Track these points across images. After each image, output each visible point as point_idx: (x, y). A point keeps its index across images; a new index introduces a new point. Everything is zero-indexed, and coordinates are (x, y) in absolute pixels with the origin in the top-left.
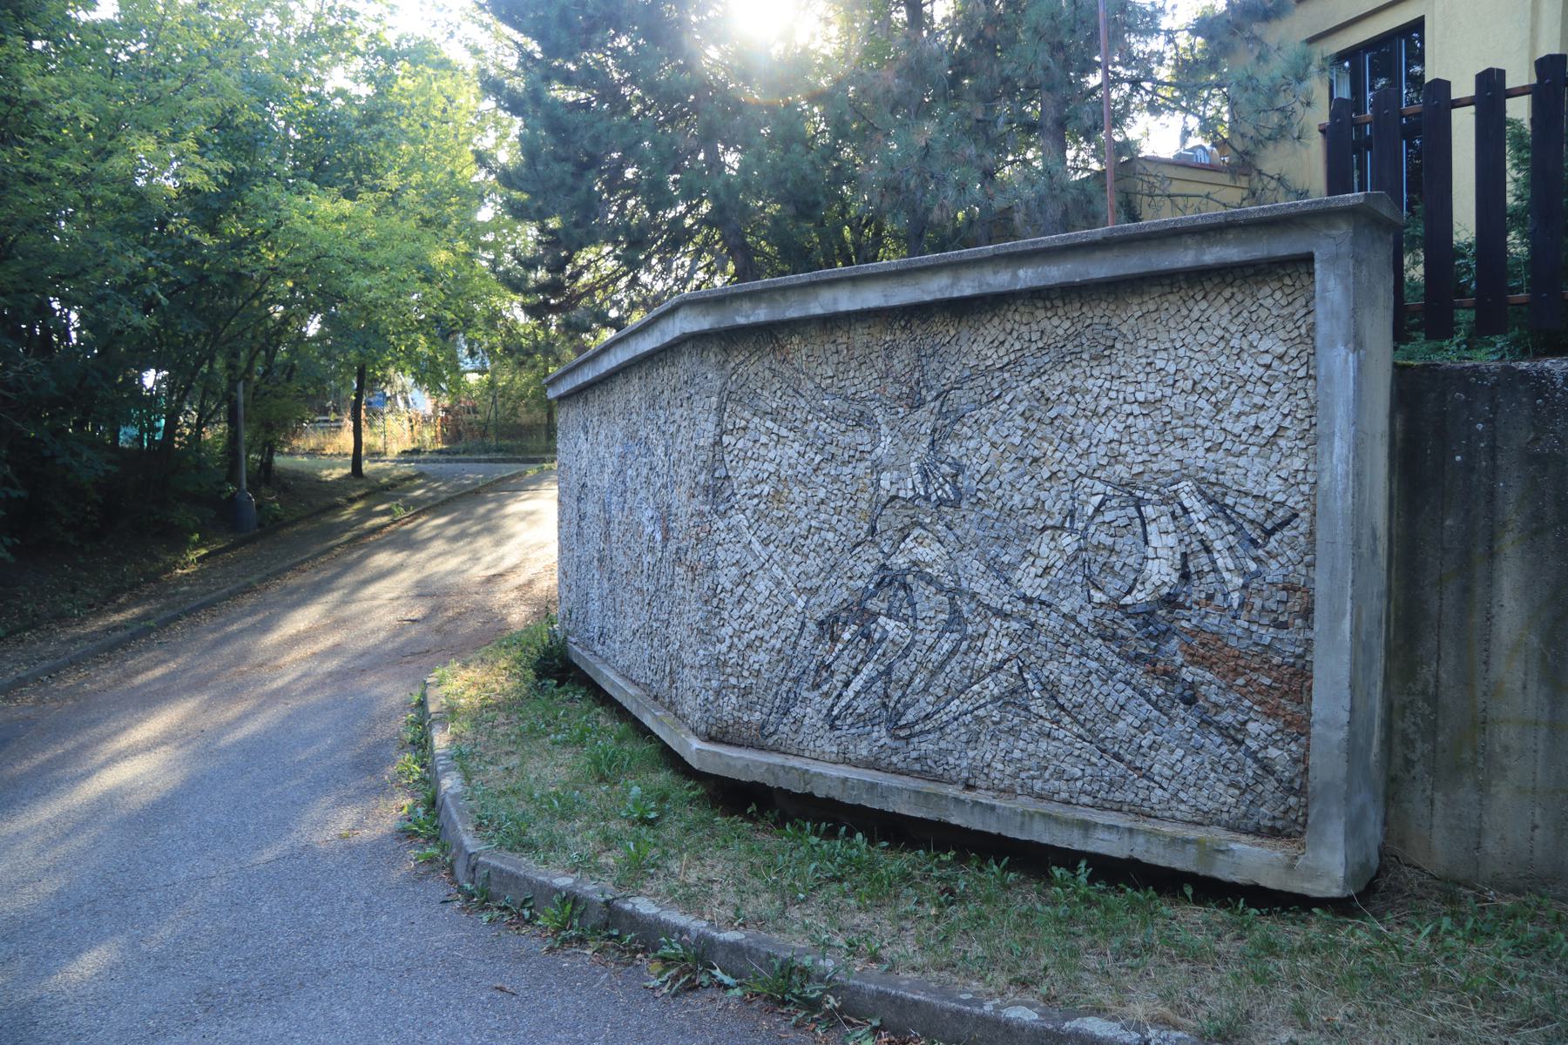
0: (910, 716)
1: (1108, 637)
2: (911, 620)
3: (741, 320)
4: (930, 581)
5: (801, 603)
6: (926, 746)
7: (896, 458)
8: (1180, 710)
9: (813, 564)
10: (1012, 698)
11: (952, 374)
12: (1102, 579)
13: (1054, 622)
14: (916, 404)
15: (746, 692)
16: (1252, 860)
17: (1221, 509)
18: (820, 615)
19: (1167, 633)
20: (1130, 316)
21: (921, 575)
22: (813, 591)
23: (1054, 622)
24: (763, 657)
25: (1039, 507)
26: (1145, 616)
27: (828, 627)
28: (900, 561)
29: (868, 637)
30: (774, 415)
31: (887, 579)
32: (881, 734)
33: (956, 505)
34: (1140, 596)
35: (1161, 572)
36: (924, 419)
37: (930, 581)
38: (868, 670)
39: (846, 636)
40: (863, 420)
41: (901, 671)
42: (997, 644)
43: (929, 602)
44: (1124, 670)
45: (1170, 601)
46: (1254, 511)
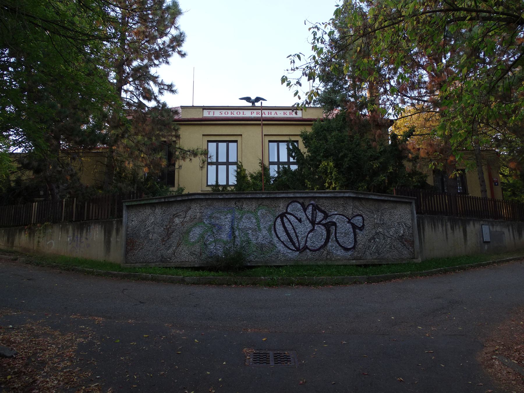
2: (380, 239)
6: (382, 255)
10: (390, 247)
14: (378, 212)
17: (406, 226)
26: (401, 237)
27: (370, 241)
31: (377, 234)
32: (377, 254)
35: (402, 232)
40: (373, 213)
45: (403, 235)
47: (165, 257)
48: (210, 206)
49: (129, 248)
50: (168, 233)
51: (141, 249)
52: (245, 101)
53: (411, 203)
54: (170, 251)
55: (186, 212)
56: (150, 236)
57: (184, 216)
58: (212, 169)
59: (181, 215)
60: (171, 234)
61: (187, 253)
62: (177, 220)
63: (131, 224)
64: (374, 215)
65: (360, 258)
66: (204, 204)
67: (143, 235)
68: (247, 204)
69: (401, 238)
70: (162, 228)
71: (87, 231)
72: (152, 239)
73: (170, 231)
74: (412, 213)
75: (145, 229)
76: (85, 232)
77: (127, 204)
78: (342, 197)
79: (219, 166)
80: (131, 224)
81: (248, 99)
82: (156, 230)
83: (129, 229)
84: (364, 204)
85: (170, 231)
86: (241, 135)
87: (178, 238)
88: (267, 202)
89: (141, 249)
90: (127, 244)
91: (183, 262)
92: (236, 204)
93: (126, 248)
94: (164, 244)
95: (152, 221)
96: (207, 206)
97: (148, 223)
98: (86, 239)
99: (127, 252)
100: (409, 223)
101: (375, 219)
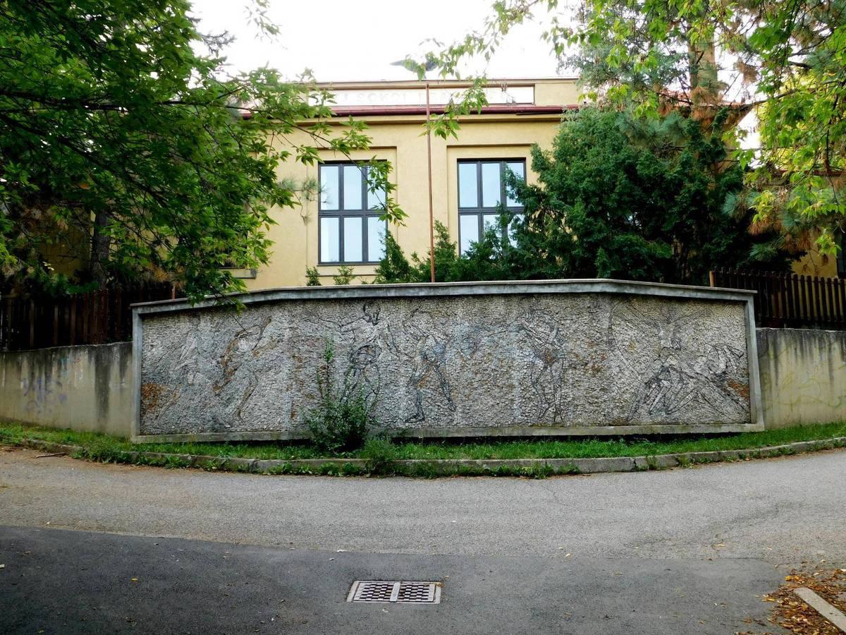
0: (671, 407)
1: (714, 382)
3: (626, 291)
4: (675, 370)
5: (640, 378)
6: (677, 414)
7: (664, 336)
8: (728, 397)
9: (643, 365)
10: (695, 399)
11: (677, 316)
12: (712, 368)
13: (703, 379)
14: (669, 323)
15: (622, 407)
16: (748, 427)
17: (732, 353)
18: (645, 381)
19: (723, 381)
20: (713, 308)
21: (672, 368)
22: (643, 374)
23: (703, 379)
24: (628, 395)
25: (698, 351)
26: (720, 376)
27: (648, 385)
28: (666, 365)
29: (659, 386)
30: (630, 321)
31: (665, 370)
32: (663, 413)
33: (680, 350)
34: (719, 372)
35: (722, 366)
36: (671, 327)
37: (675, 370)
38: (660, 396)
39: (654, 386)
40: (656, 326)
41: (668, 395)
42: (691, 385)
43: (675, 376)
44: (717, 389)
45: (724, 373)
46: (737, 353)
47: (221, 421)
49: (147, 402)
50: (227, 372)
51: (173, 404)
52: (402, 68)
53: (744, 303)
55: (262, 328)
56: (190, 377)
57: (257, 336)
58: (330, 225)
59: (251, 334)
60: (232, 373)
61: (265, 413)
62: (244, 345)
63: (149, 354)
64: (659, 331)
65: (626, 423)
66: (299, 309)
67: (174, 377)
68: (387, 310)
69: (721, 380)
70: (214, 362)
71: (60, 368)
72: (193, 385)
73: (230, 368)
74: (747, 325)
75: (179, 363)
76: (54, 369)
77: (140, 311)
78: (588, 294)
79: (346, 219)
80: (149, 354)
81: (411, 65)
82: (201, 366)
83: (147, 363)
84: (637, 307)
85: (230, 368)
86: (395, 148)
87: (246, 382)
88: (431, 306)
89: (173, 404)
90: (143, 394)
91: (256, 430)
92: (364, 309)
95: (193, 347)
96: (304, 316)
97: (185, 351)
98: (59, 384)
99: (142, 411)
100: (739, 346)
101: (660, 338)
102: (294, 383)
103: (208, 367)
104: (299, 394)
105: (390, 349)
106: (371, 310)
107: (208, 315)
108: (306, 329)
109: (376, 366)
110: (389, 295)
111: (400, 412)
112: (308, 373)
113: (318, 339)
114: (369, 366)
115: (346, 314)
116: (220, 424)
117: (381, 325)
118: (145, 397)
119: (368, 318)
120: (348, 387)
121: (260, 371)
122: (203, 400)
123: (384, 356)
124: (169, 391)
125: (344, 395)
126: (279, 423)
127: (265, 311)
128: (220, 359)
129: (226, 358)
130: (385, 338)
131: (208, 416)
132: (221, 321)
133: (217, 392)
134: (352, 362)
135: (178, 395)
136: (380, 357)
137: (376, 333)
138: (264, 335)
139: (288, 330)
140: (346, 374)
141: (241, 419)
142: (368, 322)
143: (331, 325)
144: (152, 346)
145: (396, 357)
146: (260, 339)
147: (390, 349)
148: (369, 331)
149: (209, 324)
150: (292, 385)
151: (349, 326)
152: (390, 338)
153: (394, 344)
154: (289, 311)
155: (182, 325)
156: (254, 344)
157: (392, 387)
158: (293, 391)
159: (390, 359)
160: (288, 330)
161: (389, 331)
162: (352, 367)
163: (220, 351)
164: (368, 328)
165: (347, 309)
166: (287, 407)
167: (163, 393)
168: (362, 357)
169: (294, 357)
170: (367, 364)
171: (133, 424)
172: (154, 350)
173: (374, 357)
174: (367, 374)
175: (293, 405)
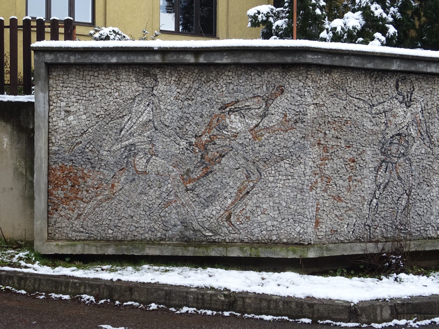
47: (196, 226)
48: (338, 87)
49: (60, 193)
50: (205, 158)
54: (215, 210)
56: (140, 162)
59: (249, 108)
60: (214, 161)
61: (274, 219)
62: (235, 123)
63: (61, 123)
66: (325, 80)
67: (111, 160)
70: (183, 143)
72: (145, 173)
73: (212, 153)
80: (61, 123)
82: (159, 146)
83: (56, 138)
85: (212, 153)
92: (397, 87)
93: (49, 193)
94: (193, 190)
95: (144, 118)
102: (319, 180)
103: (174, 149)
104: (325, 195)
105: (423, 140)
106: (404, 88)
107: (171, 75)
108: (334, 107)
109: (409, 160)
110: (429, 70)
111: (432, 218)
112: (335, 166)
113: (347, 122)
114: (402, 159)
115: (378, 91)
116: (194, 230)
117: (417, 107)
118: (57, 186)
119: (401, 98)
120: (378, 187)
121: (265, 161)
122: (164, 195)
123: (417, 148)
124: (101, 179)
125: (374, 197)
126: (299, 233)
127: (275, 77)
128: (193, 140)
129: (205, 138)
130: (418, 124)
131: (174, 218)
132: (196, 85)
133: (189, 186)
134: (383, 154)
135: (118, 186)
136: (413, 148)
137: (409, 118)
138: (271, 110)
139: (312, 107)
140: (377, 169)
141: (231, 224)
142: (401, 103)
143: (361, 104)
144: (67, 111)
145: (429, 150)
146: (264, 116)
147: (423, 140)
148: (403, 116)
149: (174, 87)
150: (316, 182)
151: (380, 107)
152: (423, 125)
153: (427, 132)
154: (313, 81)
155: (124, 86)
156: (255, 122)
157: (425, 186)
158: (318, 190)
159: (423, 152)
160: (312, 107)
161: (423, 117)
162: (383, 161)
163: (191, 128)
164: (400, 110)
165: (379, 85)
166: (310, 213)
167: (90, 182)
168: (394, 149)
169: (319, 144)
170: (399, 158)
171: (40, 224)
172: (71, 118)
173: (407, 148)
174: (400, 170)
175: (318, 209)
